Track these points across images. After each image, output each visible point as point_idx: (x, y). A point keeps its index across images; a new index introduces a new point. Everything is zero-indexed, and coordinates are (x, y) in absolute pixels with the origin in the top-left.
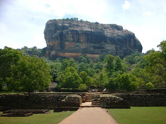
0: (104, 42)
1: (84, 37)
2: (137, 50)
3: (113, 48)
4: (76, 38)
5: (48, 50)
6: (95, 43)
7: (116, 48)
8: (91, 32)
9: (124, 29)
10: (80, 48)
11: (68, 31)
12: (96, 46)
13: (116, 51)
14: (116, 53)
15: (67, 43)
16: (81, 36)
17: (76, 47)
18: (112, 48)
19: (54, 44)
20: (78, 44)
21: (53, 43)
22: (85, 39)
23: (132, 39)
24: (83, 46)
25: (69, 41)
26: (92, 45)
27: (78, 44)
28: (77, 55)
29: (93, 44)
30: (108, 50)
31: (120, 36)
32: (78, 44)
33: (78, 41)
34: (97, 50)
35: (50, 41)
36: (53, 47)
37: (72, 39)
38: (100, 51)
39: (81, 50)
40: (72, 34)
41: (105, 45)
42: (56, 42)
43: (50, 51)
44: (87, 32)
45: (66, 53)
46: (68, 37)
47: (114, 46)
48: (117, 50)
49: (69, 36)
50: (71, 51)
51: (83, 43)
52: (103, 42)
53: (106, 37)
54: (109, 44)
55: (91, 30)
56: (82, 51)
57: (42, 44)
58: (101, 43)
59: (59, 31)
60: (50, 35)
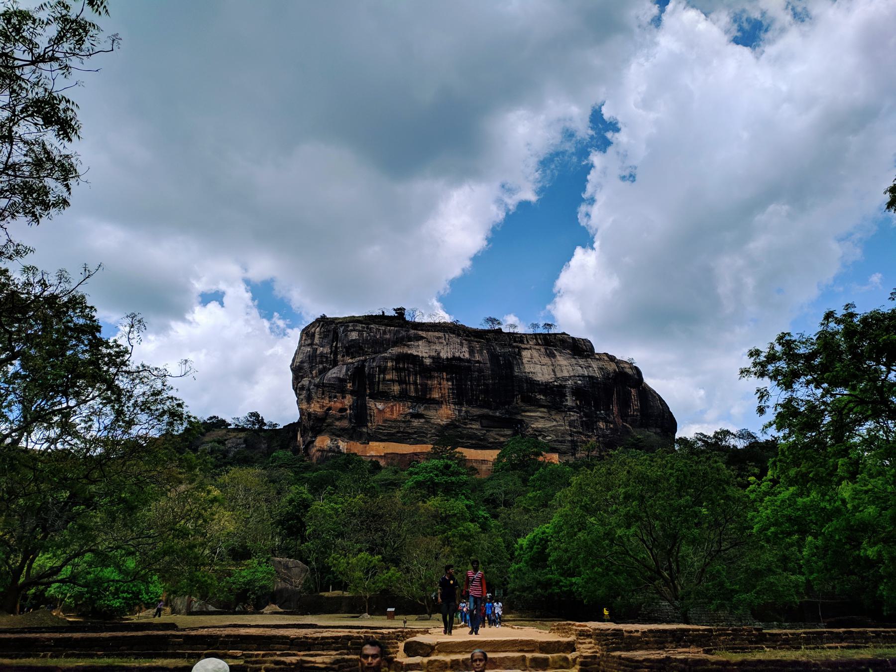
0: (522, 401)
6: (485, 405)
9: (598, 350)
10: (427, 422)
13: (571, 435)
15: (380, 406)
16: (431, 378)
17: (413, 420)
18: (555, 423)
19: (330, 409)
20: (422, 408)
22: (449, 389)
25: (384, 396)
26: (476, 411)
27: (422, 408)
28: (419, 451)
29: (481, 407)
30: (540, 432)
31: (583, 376)
33: (423, 398)
34: (492, 435)
37: (396, 388)
41: (529, 414)
49: (388, 377)
50: (393, 434)
51: (438, 403)
52: (518, 401)
53: (533, 384)
54: (544, 407)
56: (437, 436)
57: (280, 405)
60: (314, 372)
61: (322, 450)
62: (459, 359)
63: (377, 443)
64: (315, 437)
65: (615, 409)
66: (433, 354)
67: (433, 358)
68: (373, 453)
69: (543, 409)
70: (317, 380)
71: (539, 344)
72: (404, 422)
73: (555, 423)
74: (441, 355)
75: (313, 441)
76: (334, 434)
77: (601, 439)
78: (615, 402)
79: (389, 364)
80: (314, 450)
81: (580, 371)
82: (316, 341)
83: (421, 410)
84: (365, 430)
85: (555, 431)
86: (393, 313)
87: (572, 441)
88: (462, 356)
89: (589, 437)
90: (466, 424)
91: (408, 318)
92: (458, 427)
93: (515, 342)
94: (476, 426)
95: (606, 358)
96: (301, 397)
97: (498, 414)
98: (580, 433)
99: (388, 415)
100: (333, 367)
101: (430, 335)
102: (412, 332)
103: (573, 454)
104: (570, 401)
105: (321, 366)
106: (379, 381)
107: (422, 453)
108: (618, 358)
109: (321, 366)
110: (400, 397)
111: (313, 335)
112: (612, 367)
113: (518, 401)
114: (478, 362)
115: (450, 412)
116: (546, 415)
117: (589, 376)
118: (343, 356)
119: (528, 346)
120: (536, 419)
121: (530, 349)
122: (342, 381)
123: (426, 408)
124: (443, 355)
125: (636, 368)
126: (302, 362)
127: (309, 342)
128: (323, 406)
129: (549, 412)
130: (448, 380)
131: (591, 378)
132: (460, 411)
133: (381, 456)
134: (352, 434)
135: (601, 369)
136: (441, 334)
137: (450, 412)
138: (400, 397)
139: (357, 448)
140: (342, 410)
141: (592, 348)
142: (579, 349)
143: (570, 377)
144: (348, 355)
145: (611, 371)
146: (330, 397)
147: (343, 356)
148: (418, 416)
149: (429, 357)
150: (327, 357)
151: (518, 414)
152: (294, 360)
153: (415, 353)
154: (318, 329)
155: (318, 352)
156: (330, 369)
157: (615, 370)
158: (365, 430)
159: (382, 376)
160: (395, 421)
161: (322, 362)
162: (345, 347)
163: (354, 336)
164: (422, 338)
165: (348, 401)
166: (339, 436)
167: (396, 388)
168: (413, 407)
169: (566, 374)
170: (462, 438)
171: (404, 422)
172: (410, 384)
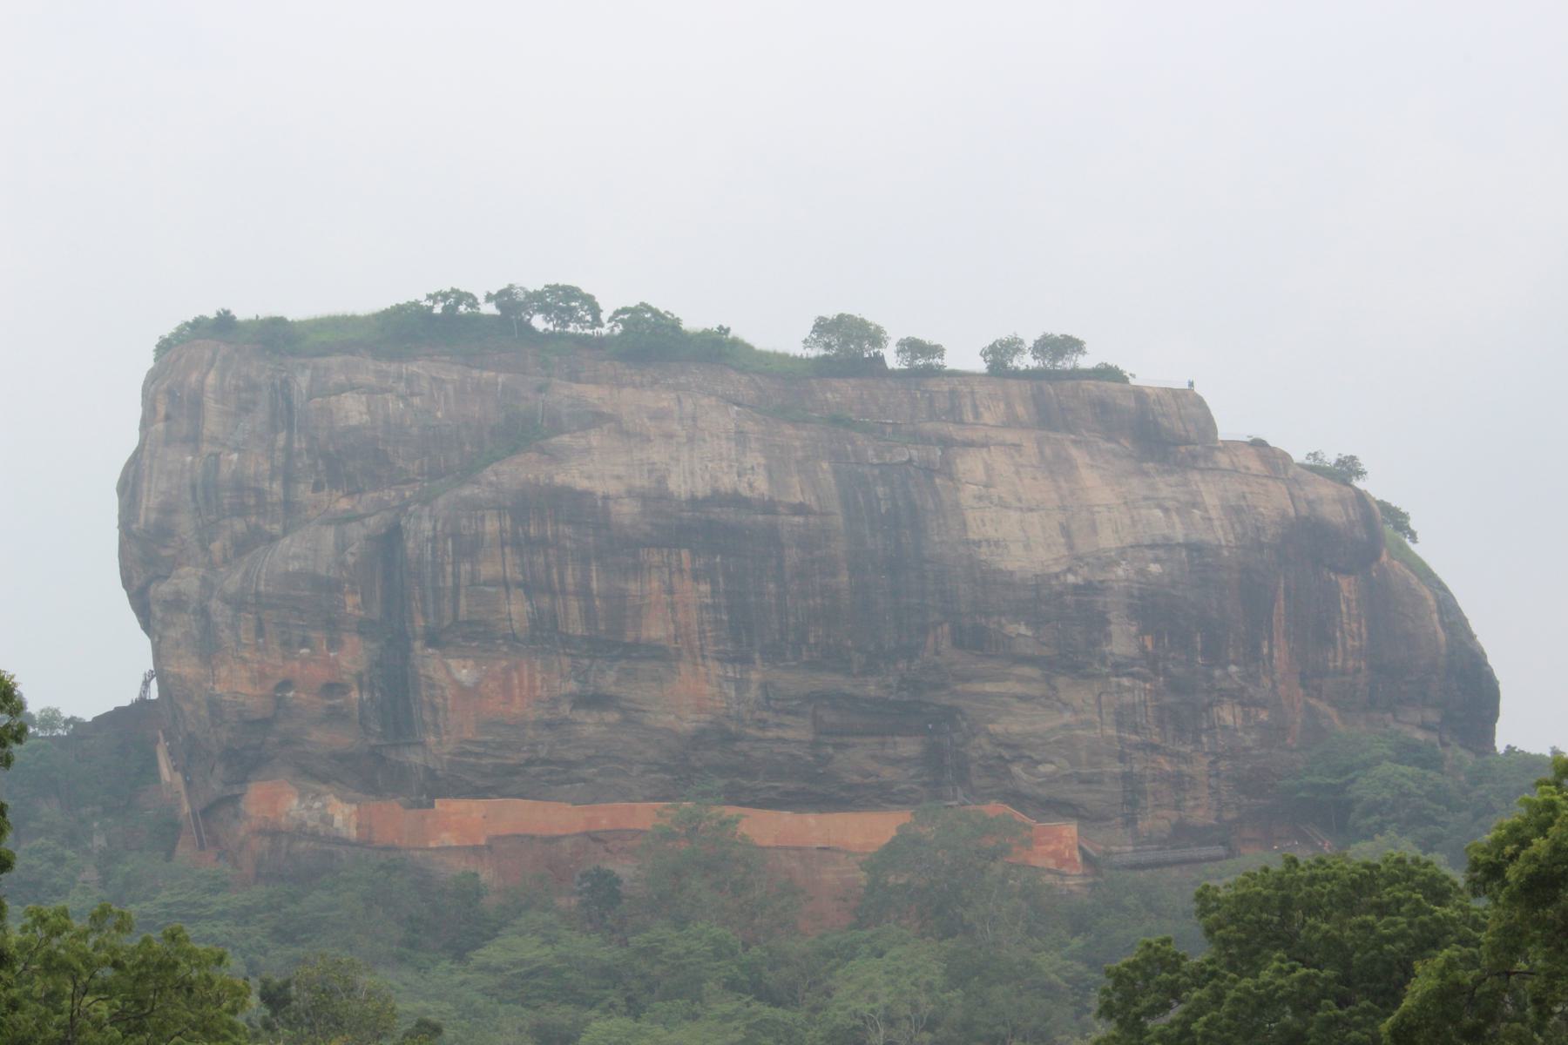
2: (1424, 726)
7: (1123, 718)
9: (1231, 425)
13: (1122, 758)
15: (465, 673)
17: (580, 715)
19: (286, 684)
20: (611, 675)
23: (1347, 586)
25: (476, 635)
27: (611, 675)
28: (604, 823)
31: (1168, 545)
38: (896, 762)
41: (976, 687)
49: (487, 570)
59: (344, 504)
60: (216, 546)
61: (274, 833)
66: (641, 482)
67: (643, 497)
68: (448, 839)
69: (1027, 671)
70: (232, 582)
71: (1011, 422)
73: (1067, 717)
75: (235, 799)
77: (1224, 765)
79: (491, 526)
81: (1158, 523)
82: (212, 424)
83: (608, 680)
84: (414, 758)
86: (489, 309)
87: (1126, 777)
88: (745, 491)
89: (1187, 759)
90: (763, 724)
94: (798, 731)
95: (1256, 466)
96: (174, 634)
97: (872, 689)
98: (1155, 748)
100: (286, 532)
101: (636, 399)
102: (565, 392)
103: (1130, 821)
104: (1122, 641)
105: (239, 525)
106: (457, 587)
108: (1299, 456)
109: (239, 525)
111: (196, 404)
112: (1273, 502)
114: (800, 509)
118: (317, 487)
119: (978, 435)
121: (985, 445)
124: (679, 485)
125: (1361, 497)
126: (167, 509)
130: (696, 577)
132: (741, 684)
133: (476, 849)
134: (369, 773)
135: (1234, 511)
136: (666, 400)
139: (395, 821)
140: (331, 688)
141: (1209, 424)
142: (1163, 432)
143: (1122, 552)
146: (286, 644)
147: (317, 487)
148: (593, 701)
149: (630, 493)
150: (259, 493)
152: (130, 486)
153: (582, 484)
154: (211, 379)
155: (225, 471)
156: (273, 539)
158: (414, 758)
159: (466, 567)
163: (353, 410)
164: (596, 419)
165: (353, 657)
166: (325, 779)
167: (517, 610)
169: (1108, 540)
171: (549, 725)
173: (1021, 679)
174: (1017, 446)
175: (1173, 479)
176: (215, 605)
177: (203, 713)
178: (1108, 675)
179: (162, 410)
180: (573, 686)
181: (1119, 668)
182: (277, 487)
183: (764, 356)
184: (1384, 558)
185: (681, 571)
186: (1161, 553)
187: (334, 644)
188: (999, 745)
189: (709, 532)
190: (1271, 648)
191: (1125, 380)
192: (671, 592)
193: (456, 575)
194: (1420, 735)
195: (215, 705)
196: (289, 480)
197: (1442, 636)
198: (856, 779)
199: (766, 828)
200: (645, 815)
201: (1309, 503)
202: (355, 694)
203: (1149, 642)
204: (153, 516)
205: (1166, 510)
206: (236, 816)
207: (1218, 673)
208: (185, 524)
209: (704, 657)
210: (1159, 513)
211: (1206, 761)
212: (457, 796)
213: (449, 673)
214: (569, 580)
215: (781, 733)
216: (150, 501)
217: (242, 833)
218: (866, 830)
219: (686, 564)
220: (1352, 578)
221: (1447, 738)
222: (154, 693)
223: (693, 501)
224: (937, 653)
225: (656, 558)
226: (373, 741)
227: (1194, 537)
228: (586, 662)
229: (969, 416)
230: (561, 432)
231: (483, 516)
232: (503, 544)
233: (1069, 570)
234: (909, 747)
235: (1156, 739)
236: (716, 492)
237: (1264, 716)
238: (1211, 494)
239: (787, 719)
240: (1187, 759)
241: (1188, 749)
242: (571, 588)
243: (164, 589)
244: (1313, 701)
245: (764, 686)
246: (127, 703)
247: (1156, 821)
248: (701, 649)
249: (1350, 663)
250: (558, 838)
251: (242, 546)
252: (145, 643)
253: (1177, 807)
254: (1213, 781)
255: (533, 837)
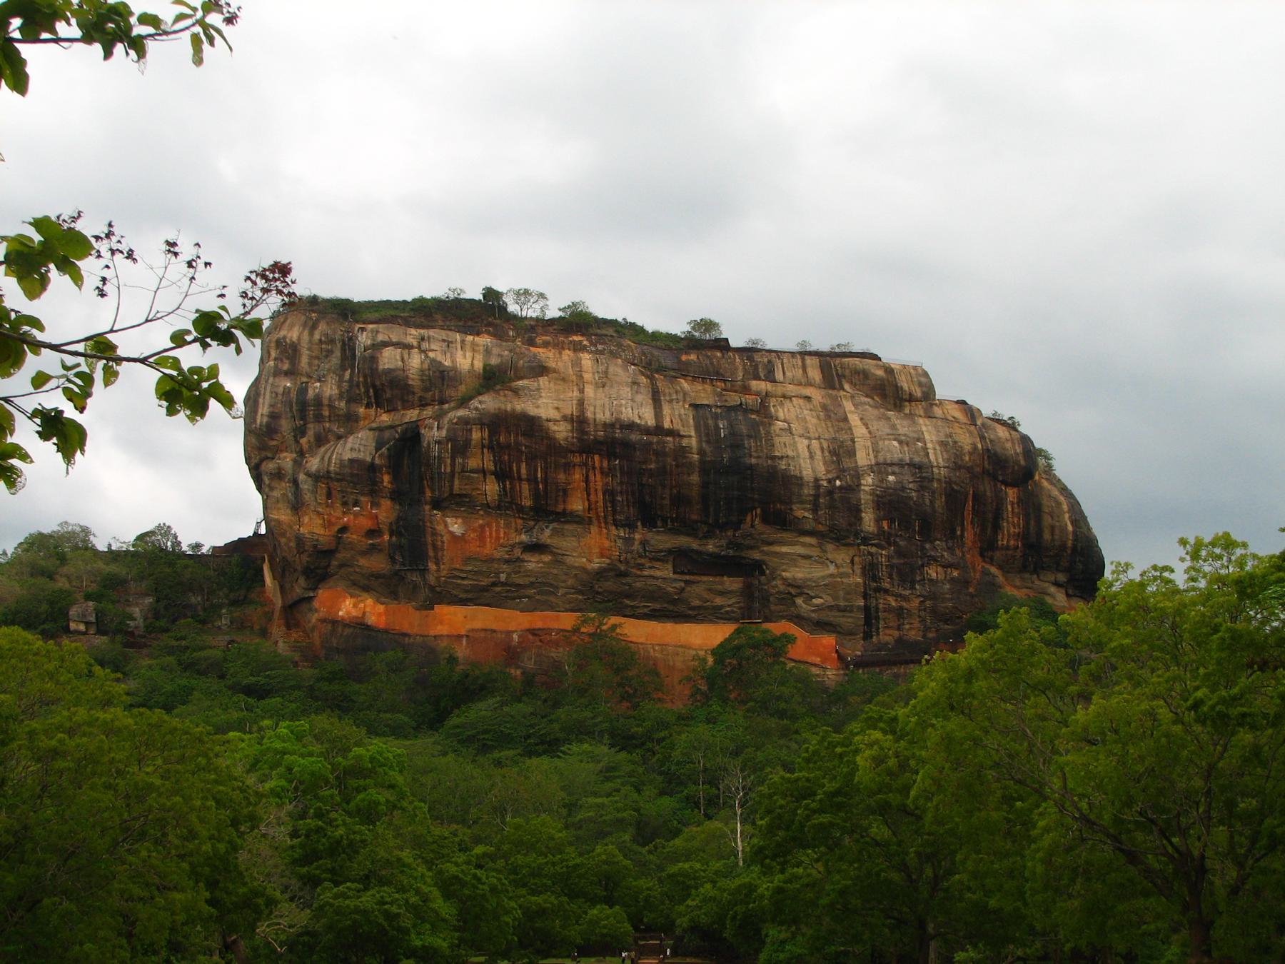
0: (765, 520)
1: (598, 481)
2: (1057, 584)
3: (847, 575)
4: (532, 480)
5: (280, 576)
6: (684, 526)
7: (870, 570)
8: (659, 430)
9: (943, 391)
11: (465, 422)
12: (699, 553)
13: (865, 596)
14: (866, 609)
15: (456, 527)
16: (568, 467)
17: (526, 557)
18: (832, 569)
19: (344, 529)
20: (548, 532)
21: (328, 524)
23: (1011, 494)
24: (588, 549)
26: (662, 540)
27: (548, 532)
28: (539, 625)
30: (799, 588)
31: (901, 464)
32: (546, 535)
33: (546, 508)
35: (308, 497)
36: (329, 553)
37: (492, 488)
39: (570, 582)
40: (492, 446)
41: (777, 549)
42: (356, 515)
43: (302, 581)
44: (618, 434)
45: (443, 610)
46: (458, 469)
47: (852, 551)
48: (878, 590)
49: (473, 463)
50: (485, 589)
52: (754, 523)
55: (658, 414)
58: (737, 529)
60: (304, 441)
62: (631, 426)
63: (452, 608)
64: (315, 589)
65: (969, 535)
68: (442, 630)
69: (808, 540)
70: (314, 464)
72: (507, 562)
74: (589, 415)
75: (310, 599)
76: (355, 584)
77: (928, 603)
78: (968, 515)
80: (314, 618)
81: (894, 451)
82: (304, 361)
83: (546, 536)
85: (831, 587)
89: (905, 598)
90: (641, 567)
91: (513, 308)
92: (625, 574)
93: (757, 378)
95: (959, 415)
96: (276, 494)
97: (711, 547)
98: (886, 591)
99: (473, 548)
103: (867, 636)
104: (868, 520)
106: (453, 473)
107: (548, 631)
110: (499, 507)
113: (754, 523)
115: (607, 544)
116: (814, 552)
117: (911, 465)
118: (368, 406)
120: (793, 559)
122: (372, 468)
123: (555, 532)
125: (1025, 440)
126: (274, 416)
127: (286, 367)
128: (330, 524)
129: (820, 545)
131: (919, 469)
132: (628, 541)
135: (942, 444)
137: (607, 544)
138: (499, 507)
140: (372, 533)
144: (379, 405)
145: (968, 448)
146: (345, 504)
149: (565, 418)
151: (751, 548)
153: (532, 411)
155: (311, 394)
156: (339, 437)
157: (975, 448)
159: (459, 460)
160: (491, 560)
161: (319, 418)
162: (374, 386)
163: (389, 359)
165: (386, 512)
166: (366, 589)
168: (529, 530)
170: (629, 596)
171: (507, 562)
172: (520, 479)
173: (804, 545)
174: (808, 398)
175: (905, 423)
176: (302, 477)
177: (293, 544)
178: (859, 545)
179: (273, 354)
180: (524, 537)
181: (866, 541)
182: (343, 404)
183: (656, 336)
184: (1037, 477)
185: (594, 468)
186: (896, 469)
187: (375, 504)
188: (789, 585)
189: (611, 445)
190: (962, 531)
191: (879, 359)
192: (587, 480)
193: (453, 464)
194: (1053, 589)
195: (300, 540)
196: (352, 399)
197: (1070, 528)
198: (697, 603)
199: (640, 632)
200: (567, 620)
201: (991, 441)
202: (386, 537)
203: (885, 525)
204: (265, 420)
205: (900, 442)
206: (310, 610)
207: (928, 546)
208: (285, 426)
209: (606, 523)
210: (895, 443)
211: (918, 601)
212: (449, 604)
213: (446, 526)
214: (524, 471)
215: (652, 572)
216: (264, 410)
217: (314, 621)
218: (704, 637)
219: (597, 464)
220: (1016, 490)
221: (1070, 592)
222: (263, 531)
223: (606, 426)
224: (752, 526)
225: (577, 459)
226: (397, 567)
227: (917, 459)
228: (532, 523)
229: (779, 376)
230: (521, 378)
231: (471, 430)
232: (483, 447)
233: (838, 478)
234: (733, 584)
235: (887, 586)
236: (618, 420)
237: (955, 574)
238: (930, 433)
239: (657, 564)
240: (905, 598)
241: (907, 592)
242: (524, 476)
243: (270, 466)
244: (987, 566)
245: (644, 543)
246: (246, 536)
247: (887, 636)
248: (605, 517)
249: (1012, 542)
250: (509, 633)
251: (320, 441)
252: (257, 499)
253: (899, 629)
254: (922, 613)
255: (495, 631)
